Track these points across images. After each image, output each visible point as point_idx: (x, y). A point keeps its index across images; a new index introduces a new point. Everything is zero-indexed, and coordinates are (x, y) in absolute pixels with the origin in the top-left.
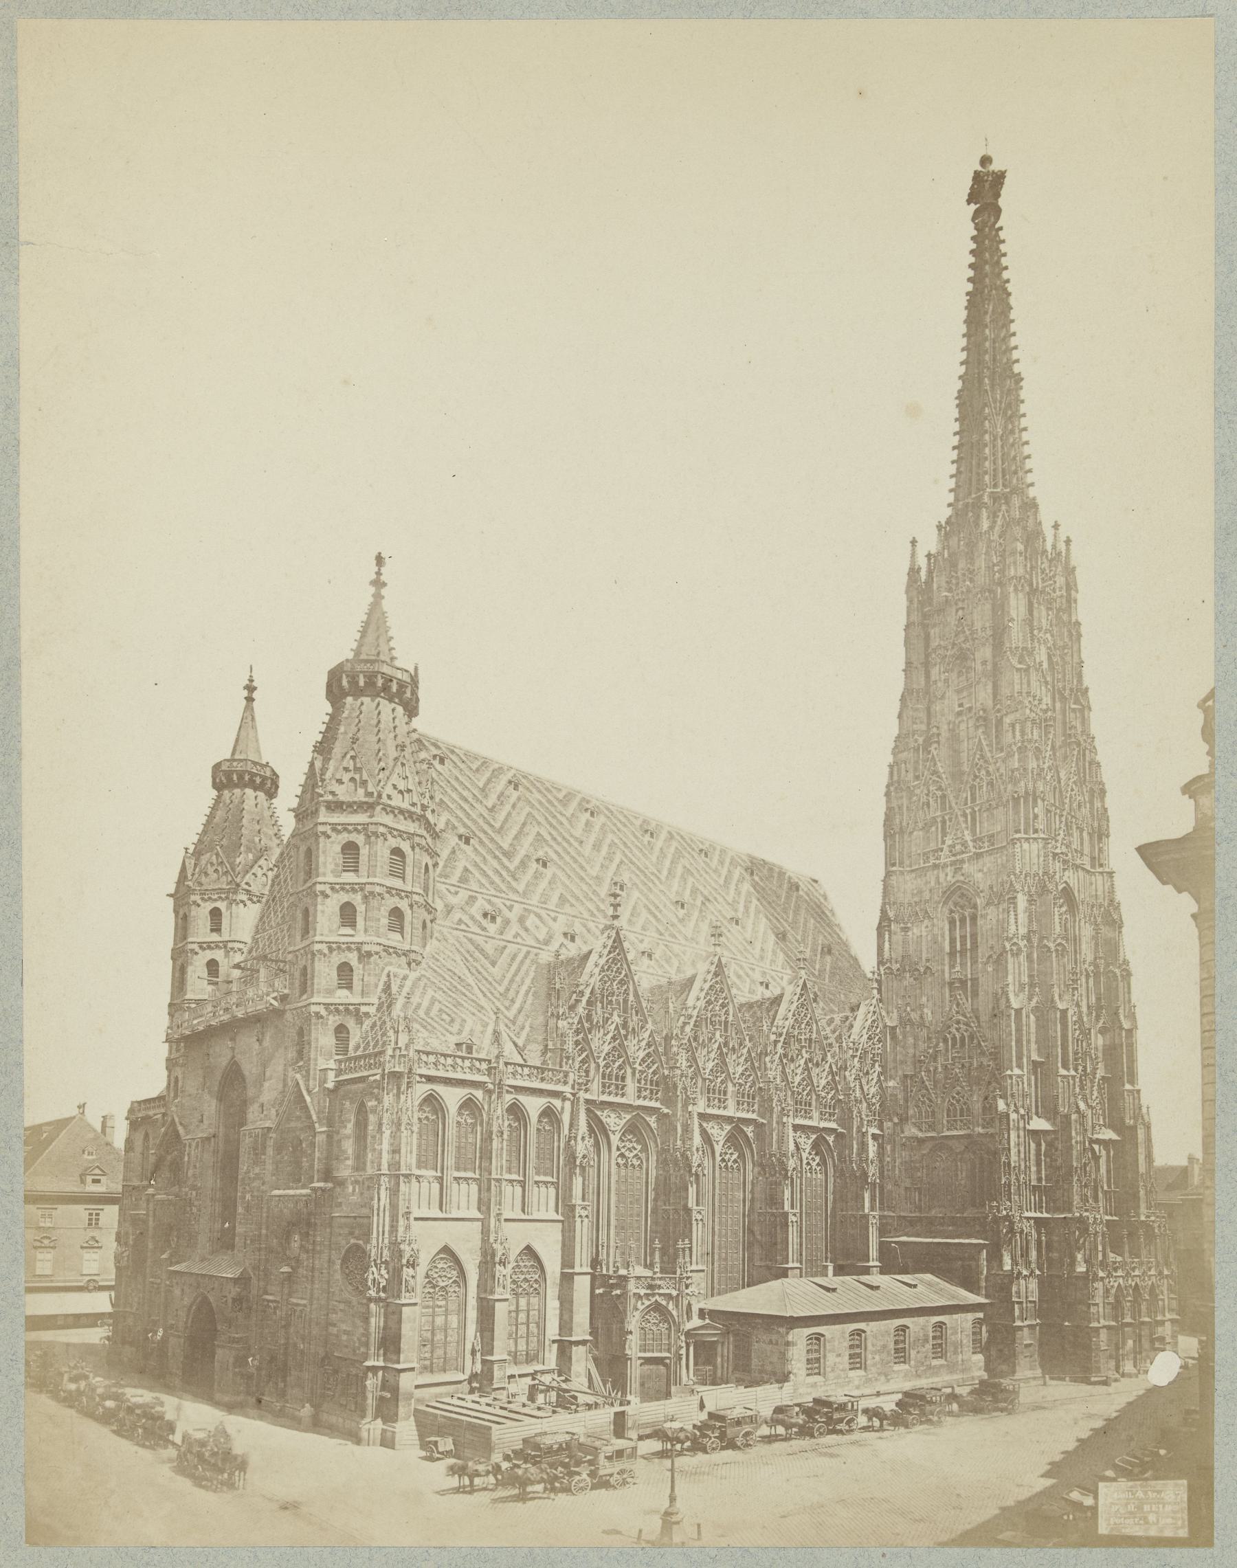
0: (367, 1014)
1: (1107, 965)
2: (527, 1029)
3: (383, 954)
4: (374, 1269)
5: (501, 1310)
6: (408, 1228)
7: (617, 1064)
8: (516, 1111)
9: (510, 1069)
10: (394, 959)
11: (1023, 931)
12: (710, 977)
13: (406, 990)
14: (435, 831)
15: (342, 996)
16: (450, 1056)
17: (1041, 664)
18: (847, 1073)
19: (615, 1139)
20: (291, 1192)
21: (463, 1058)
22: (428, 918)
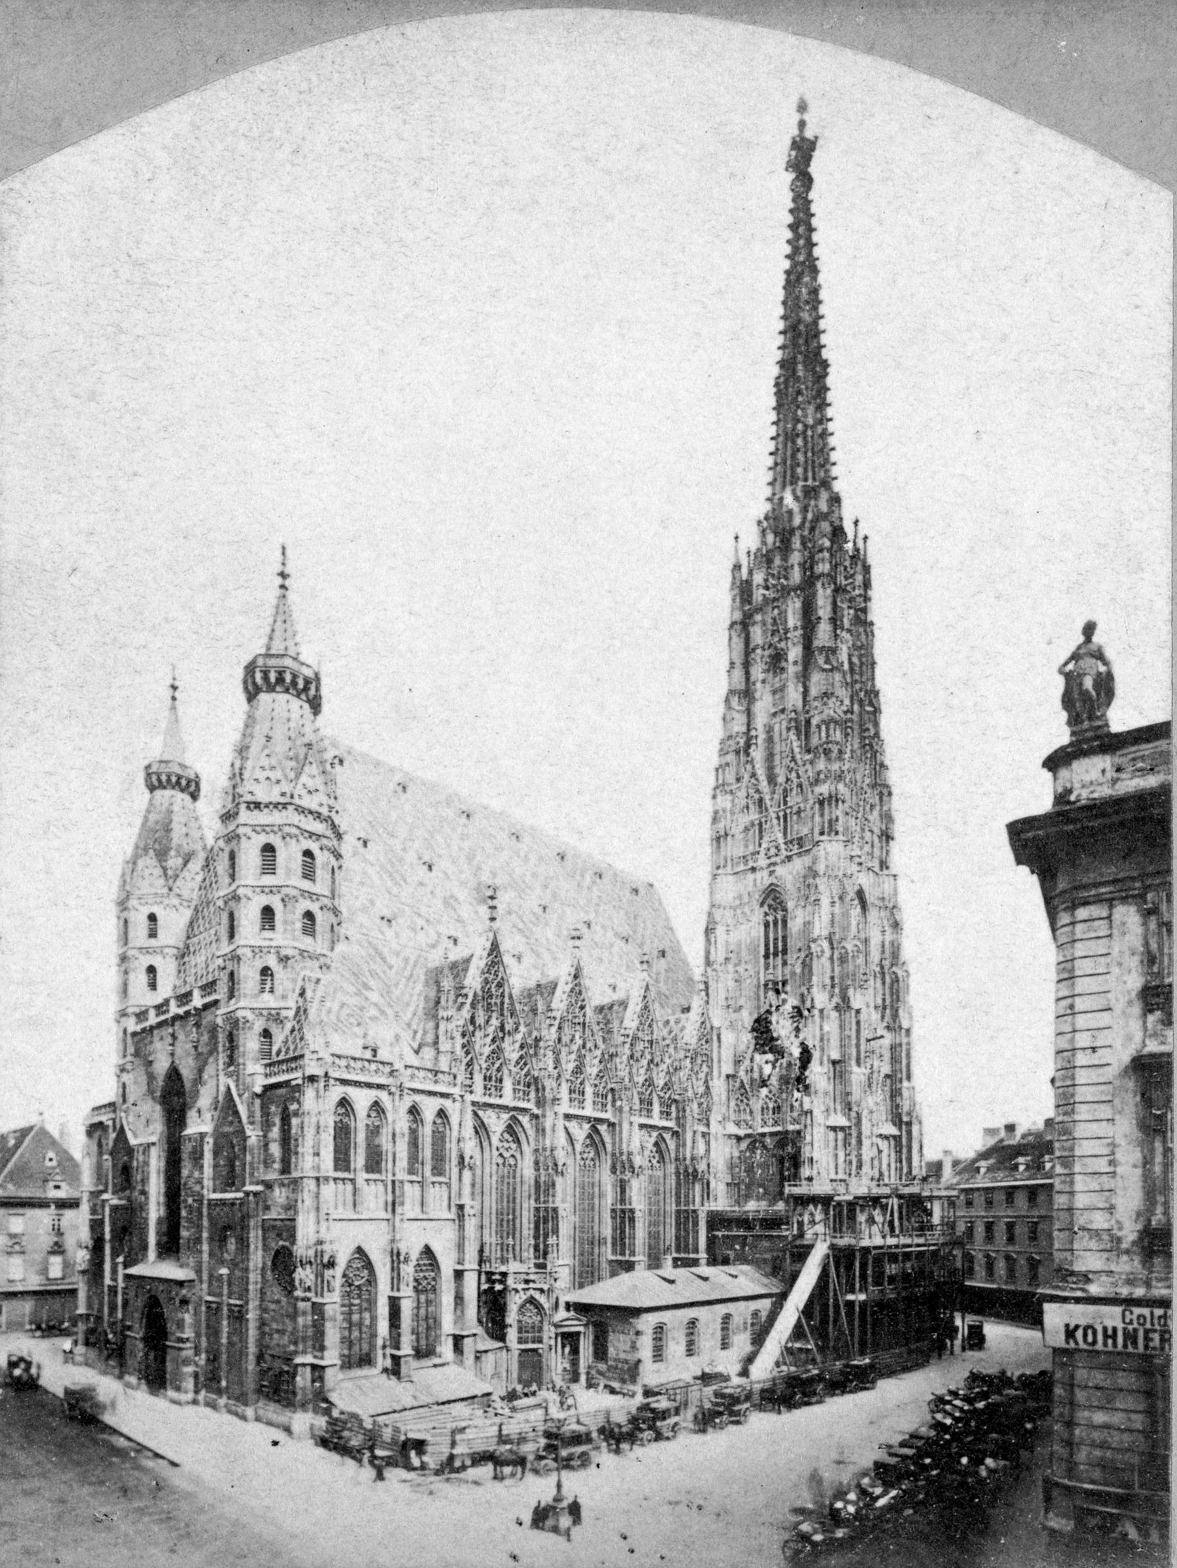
0: (286, 1018)
3: (298, 958)
7: (497, 1065)
8: (414, 1111)
9: (409, 1071)
10: (309, 963)
11: (825, 933)
12: (570, 979)
13: (319, 993)
17: (842, 664)
19: (495, 1140)
21: (369, 1061)
22: (335, 921)
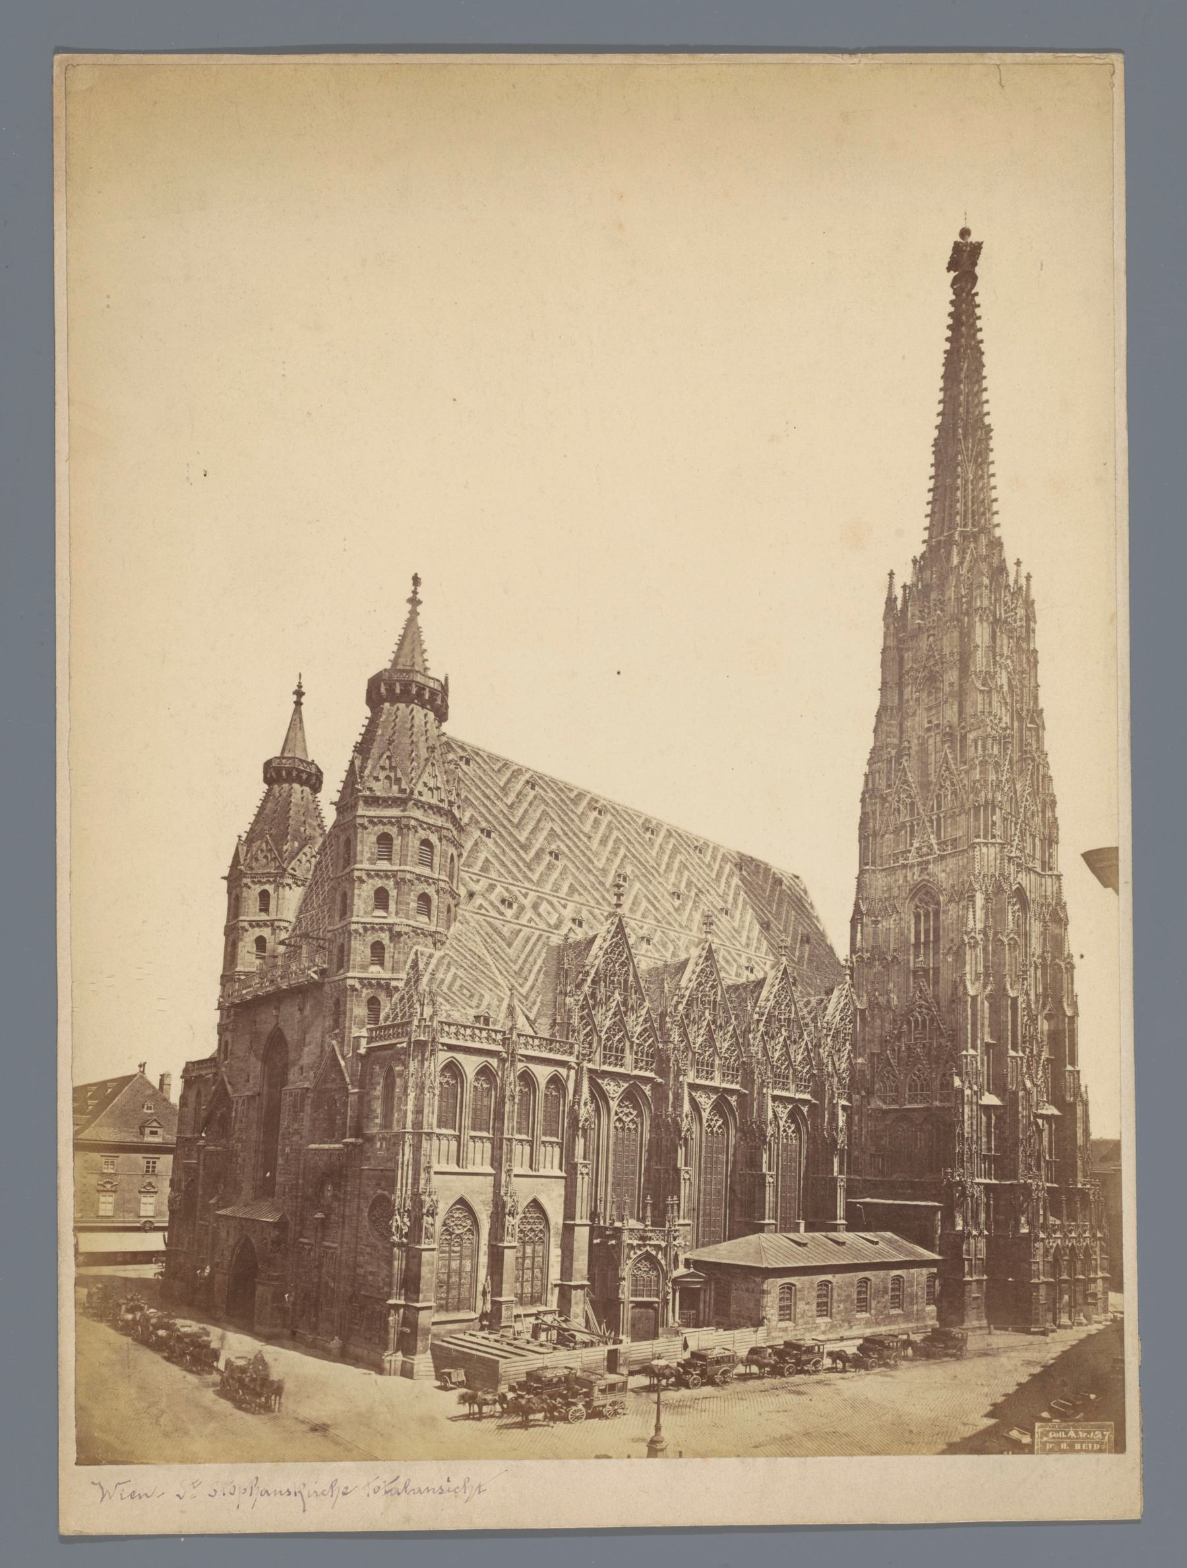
0: (396, 989)
1: (1054, 958)
2: (538, 1004)
3: (412, 934)
4: (398, 1217)
5: (509, 1257)
6: (428, 1181)
7: (617, 1038)
8: (527, 1078)
9: (522, 1040)
10: (421, 939)
11: (980, 926)
12: (701, 961)
13: (431, 967)
14: (461, 826)
15: (375, 971)
16: (469, 1027)
17: (1001, 687)
18: (821, 1051)
19: (614, 1105)
20: (326, 1146)
22: (452, 902)
